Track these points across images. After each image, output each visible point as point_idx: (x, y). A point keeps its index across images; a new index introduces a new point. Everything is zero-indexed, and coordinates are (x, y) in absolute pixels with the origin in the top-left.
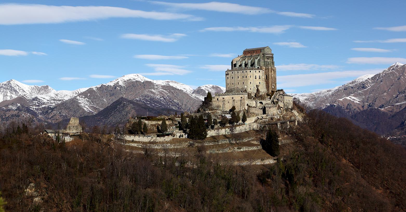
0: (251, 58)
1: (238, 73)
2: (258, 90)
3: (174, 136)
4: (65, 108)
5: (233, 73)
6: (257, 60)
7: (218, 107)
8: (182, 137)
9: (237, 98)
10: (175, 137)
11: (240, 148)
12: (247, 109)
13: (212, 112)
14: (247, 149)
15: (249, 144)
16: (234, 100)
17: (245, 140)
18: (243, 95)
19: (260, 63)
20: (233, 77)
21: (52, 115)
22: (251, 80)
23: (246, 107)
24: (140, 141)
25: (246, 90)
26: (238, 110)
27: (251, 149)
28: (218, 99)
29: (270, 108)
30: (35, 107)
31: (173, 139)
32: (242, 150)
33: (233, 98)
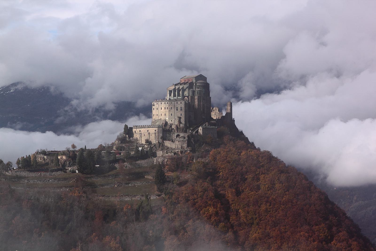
1: (161, 104)
5: (157, 104)
11: (129, 183)
18: (157, 128)
20: (157, 108)
33: (148, 131)
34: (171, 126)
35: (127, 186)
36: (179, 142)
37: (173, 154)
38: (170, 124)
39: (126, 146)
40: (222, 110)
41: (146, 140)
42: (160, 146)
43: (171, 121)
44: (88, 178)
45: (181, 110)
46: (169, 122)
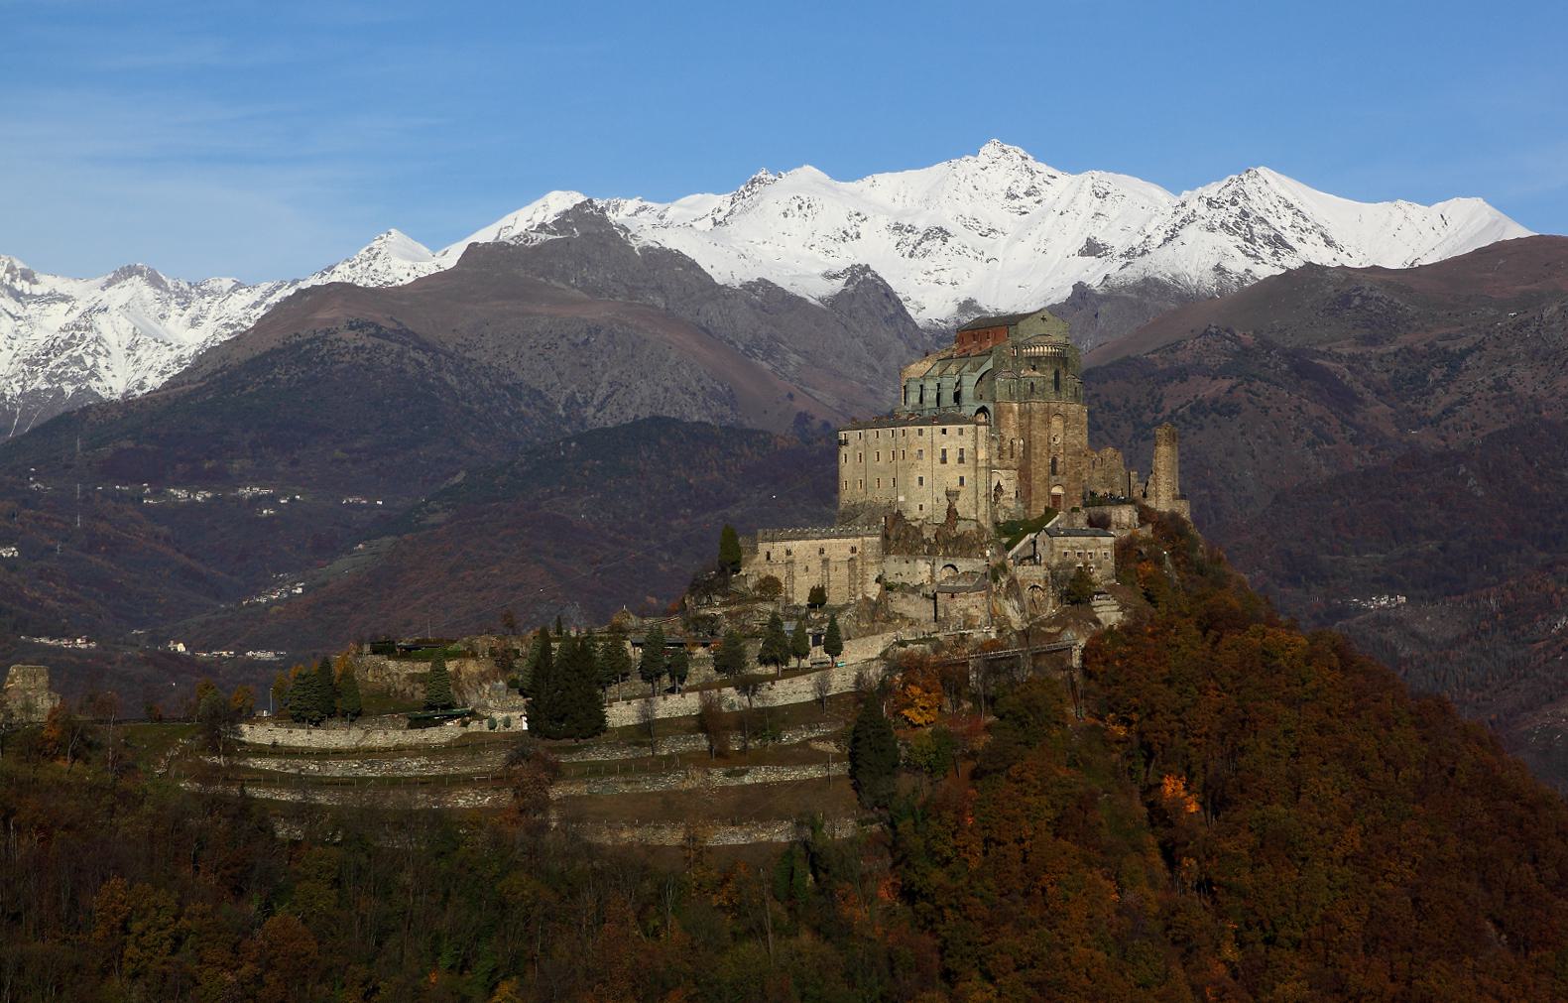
0: (965, 365)
2: (952, 512)
3: (465, 724)
4: (1536, 351)
6: (977, 375)
7: (770, 587)
8: (507, 723)
9: (839, 548)
10: (474, 727)
11: (745, 772)
12: (875, 598)
13: (729, 615)
14: (773, 777)
15: (804, 755)
16: (826, 561)
17: (788, 737)
18: (860, 539)
19: (992, 389)
21: (1446, 400)
22: (927, 465)
23: (874, 591)
24: (313, 745)
25: (899, 512)
26: (841, 603)
27: (792, 774)
28: (768, 553)
29: (953, 597)
30: (1346, 351)
31: (465, 735)
32: (747, 780)
33: (822, 551)
34: (918, 531)
35: (734, 782)
36: (953, 597)
37: (927, 647)
38: (917, 519)
39: (729, 615)
40: (601, 705)
41: (813, 589)
42: (874, 613)
43: (921, 507)
44: (571, 750)
45: (959, 462)
46: (913, 513)
